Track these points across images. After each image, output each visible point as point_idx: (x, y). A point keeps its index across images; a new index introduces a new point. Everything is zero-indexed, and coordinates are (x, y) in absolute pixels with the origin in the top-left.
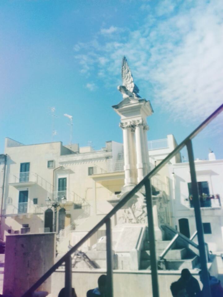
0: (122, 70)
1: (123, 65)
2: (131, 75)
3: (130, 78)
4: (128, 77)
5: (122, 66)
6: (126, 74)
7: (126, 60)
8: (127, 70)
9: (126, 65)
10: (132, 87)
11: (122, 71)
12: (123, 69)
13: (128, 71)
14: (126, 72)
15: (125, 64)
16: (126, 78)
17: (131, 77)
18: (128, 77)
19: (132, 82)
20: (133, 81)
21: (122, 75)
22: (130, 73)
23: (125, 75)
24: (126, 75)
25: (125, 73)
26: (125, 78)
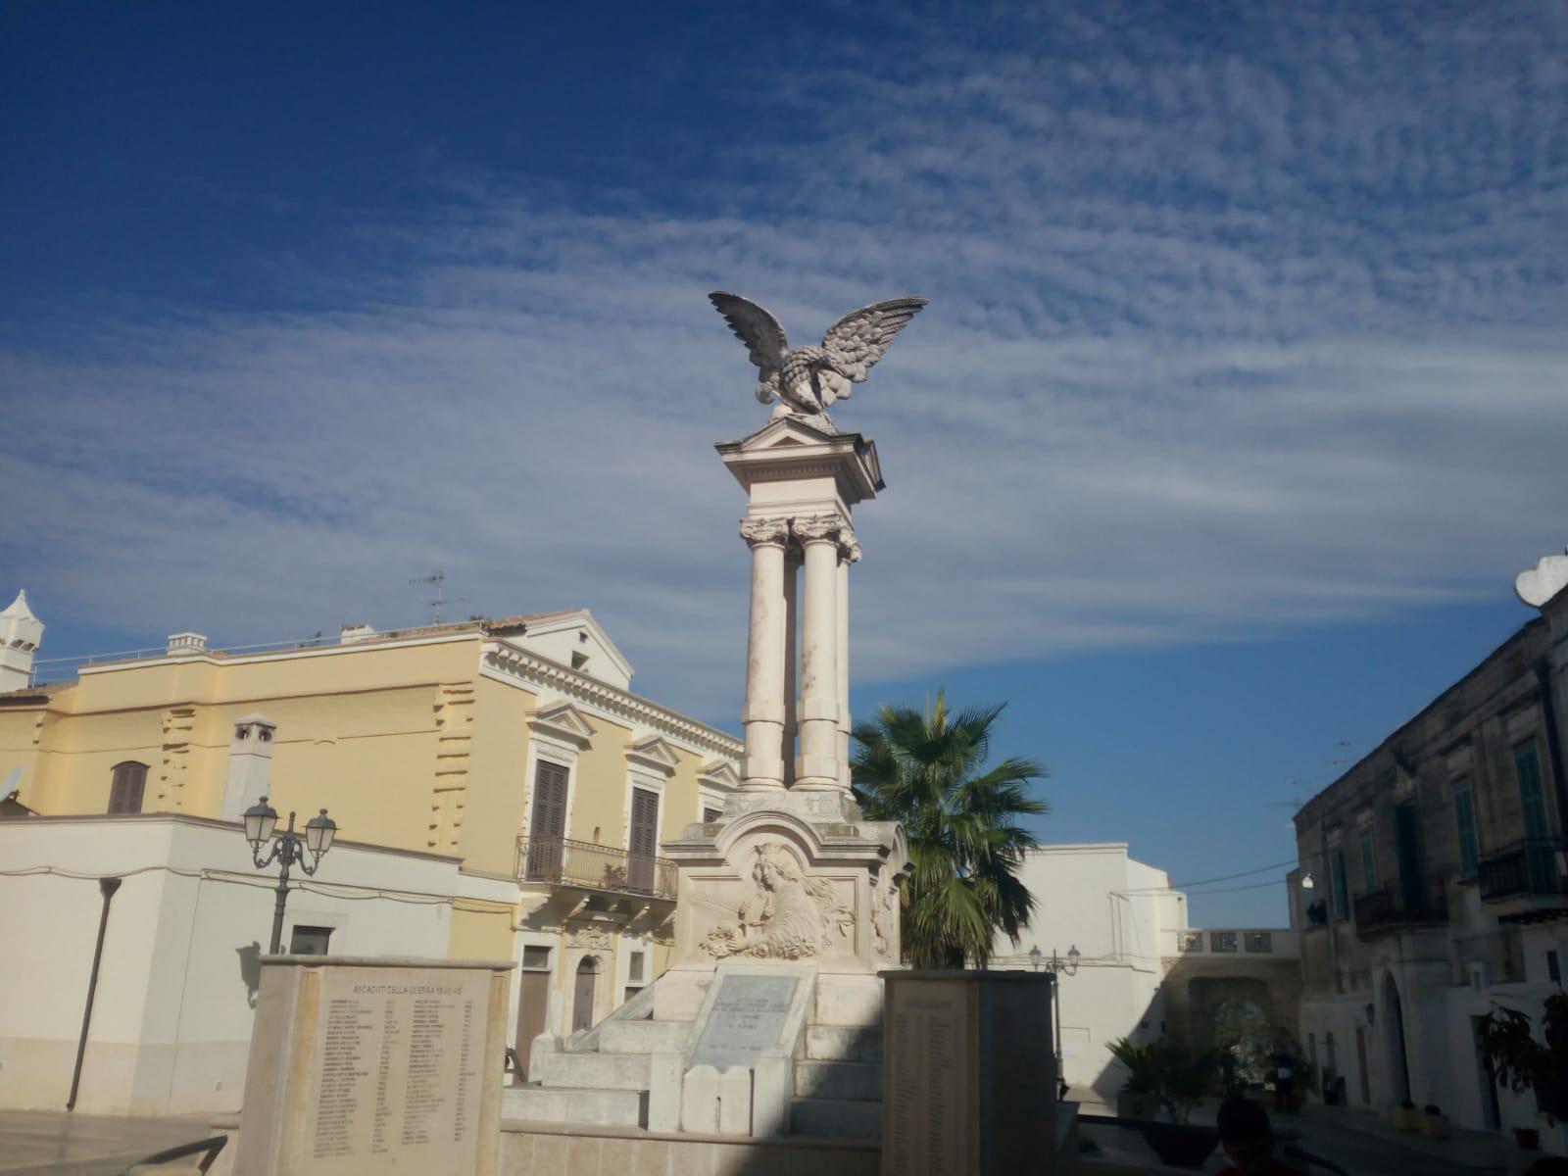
0: (866, 311)
1: (883, 311)
2: (873, 358)
3: (858, 360)
4: (854, 349)
5: (880, 307)
6: (861, 336)
7: (910, 315)
8: (877, 336)
9: (892, 321)
10: (835, 391)
11: (861, 315)
12: (871, 311)
13: (876, 342)
14: (866, 332)
15: (898, 315)
16: (843, 341)
17: (866, 362)
18: (854, 349)
19: (851, 377)
20: (858, 377)
21: (847, 320)
22: (874, 348)
23: (853, 335)
24: (856, 338)
25: (862, 331)
26: (841, 338)
